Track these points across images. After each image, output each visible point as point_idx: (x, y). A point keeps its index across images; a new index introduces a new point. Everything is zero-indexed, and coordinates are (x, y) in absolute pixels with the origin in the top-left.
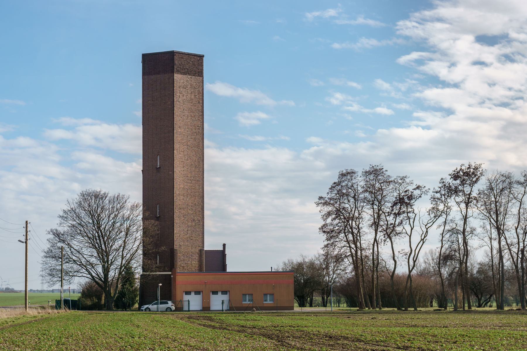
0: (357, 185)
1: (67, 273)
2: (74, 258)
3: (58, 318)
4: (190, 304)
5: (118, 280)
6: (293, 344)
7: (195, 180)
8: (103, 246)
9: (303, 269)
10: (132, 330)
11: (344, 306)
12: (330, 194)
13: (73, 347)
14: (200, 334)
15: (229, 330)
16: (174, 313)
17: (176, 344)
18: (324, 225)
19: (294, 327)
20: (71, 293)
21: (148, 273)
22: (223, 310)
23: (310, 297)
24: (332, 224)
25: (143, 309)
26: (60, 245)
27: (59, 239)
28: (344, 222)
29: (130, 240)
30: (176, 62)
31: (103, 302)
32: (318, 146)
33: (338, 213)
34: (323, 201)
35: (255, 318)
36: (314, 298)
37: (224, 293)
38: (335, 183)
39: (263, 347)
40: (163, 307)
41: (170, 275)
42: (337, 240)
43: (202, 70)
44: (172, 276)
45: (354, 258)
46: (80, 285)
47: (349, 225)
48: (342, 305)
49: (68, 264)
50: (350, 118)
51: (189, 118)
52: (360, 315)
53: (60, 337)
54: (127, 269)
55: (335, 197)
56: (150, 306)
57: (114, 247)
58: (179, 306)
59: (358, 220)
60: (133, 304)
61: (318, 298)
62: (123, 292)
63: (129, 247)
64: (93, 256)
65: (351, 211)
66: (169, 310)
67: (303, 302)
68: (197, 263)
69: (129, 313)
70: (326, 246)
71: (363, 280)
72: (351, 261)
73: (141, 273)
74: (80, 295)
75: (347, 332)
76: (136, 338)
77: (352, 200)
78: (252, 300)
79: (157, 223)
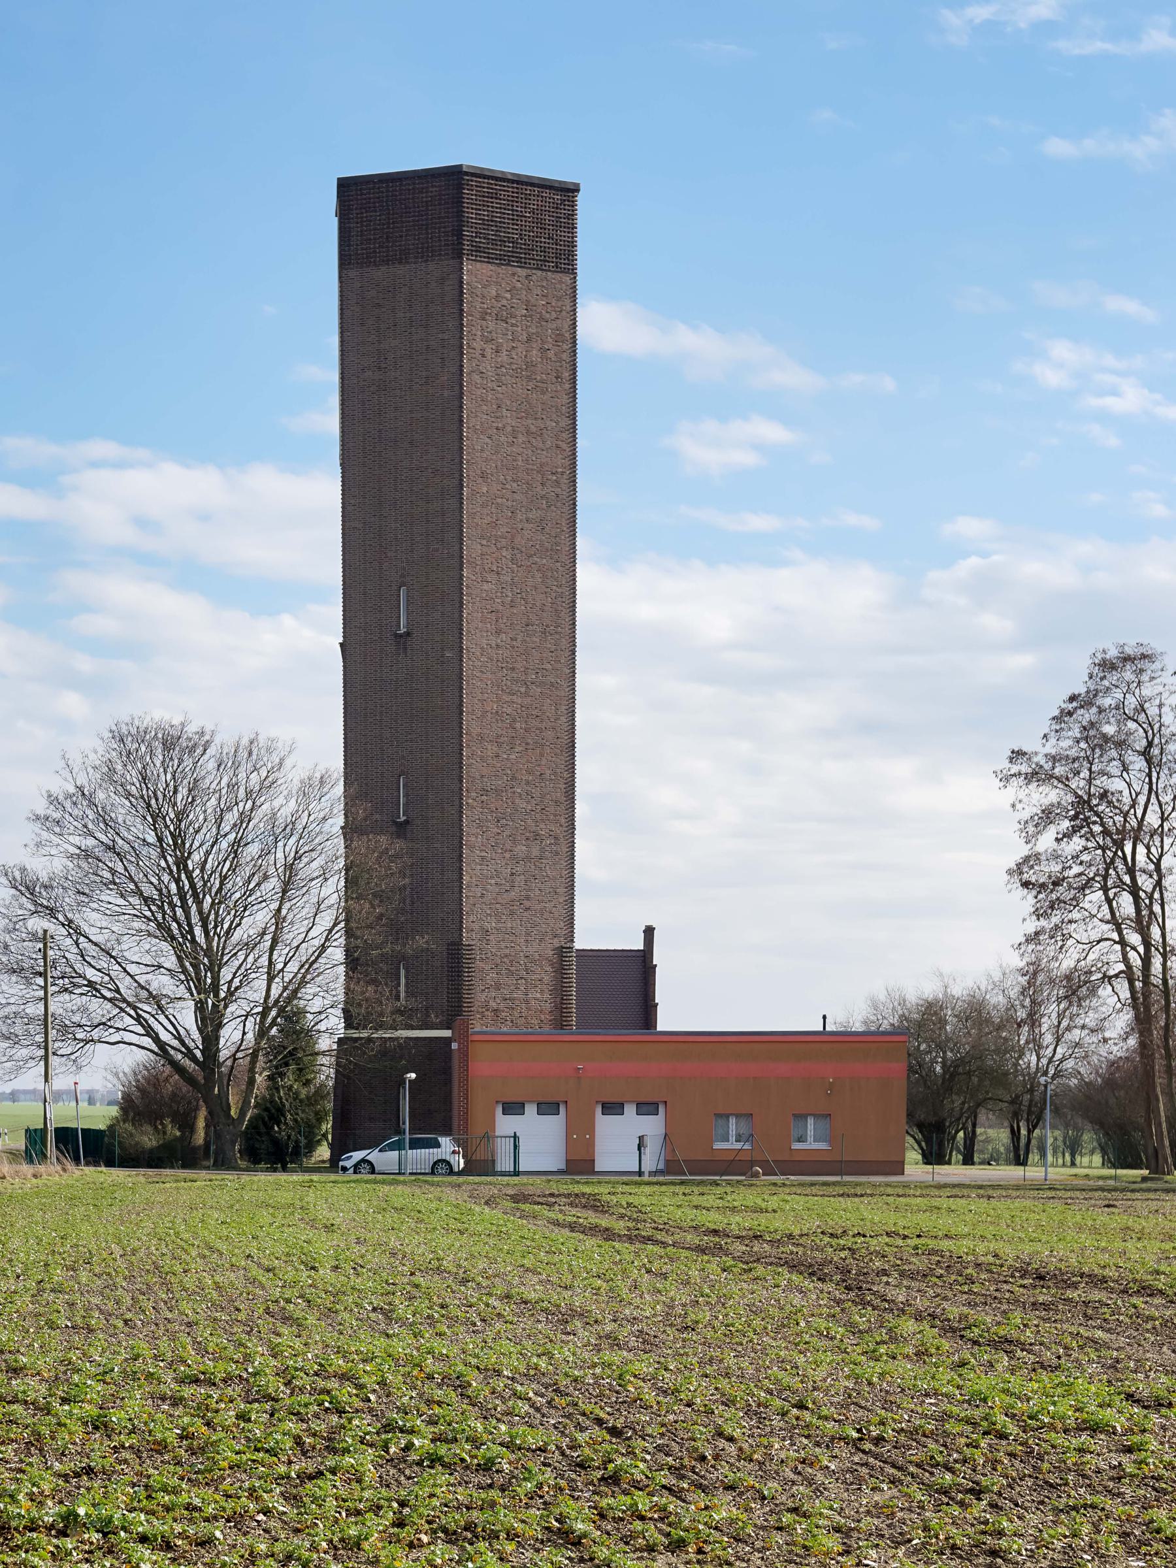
0: (1160, 706)
1: (64, 1029)
2: (91, 974)
3: (37, 1195)
4: (522, 1149)
5: (254, 1056)
6: (901, 1298)
7: (542, 684)
8: (198, 931)
9: (943, 1022)
10: (308, 1242)
11: (1092, 1164)
12: (1053, 741)
13: (96, 1300)
14: (556, 1258)
15: (664, 1244)
16: (461, 1179)
17: (470, 1292)
18: (1027, 859)
19: (905, 1237)
20: (83, 1104)
21: (364, 1034)
22: (640, 1173)
23: (964, 1128)
24: (1056, 856)
25: (348, 1164)
26: (38, 924)
27: (35, 903)
28: (1104, 849)
29: (300, 910)
30: (470, 214)
31: (200, 1137)
32: (985, 555)
33: (1083, 813)
34: (1024, 768)
35: (759, 1201)
36: (979, 1131)
37: (646, 1108)
38: (1073, 698)
39: (788, 1308)
40: (421, 1157)
41: (447, 1041)
42: (1075, 915)
43: (572, 244)
44: (454, 1046)
45: (1139, 985)
46: (116, 1075)
47: (1124, 858)
48: (1086, 1160)
49: (66, 996)
50: (1113, 441)
51: (521, 438)
52: (1151, 1195)
53: (47, 1265)
54: (288, 1019)
55: (1073, 753)
56: (374, 1156)
57: (237, 935)
58: (479, 1155)
59: (1157, 839)
60: (311, 1147)
61: (994, 1134)
62: (272, 1101)
63: (292, 935)
64: (160, 967)
65: (1133, 806)
66: (442, 1168)
67: (941, 1144)
68: (547, 996)
69: (295, 1177)
70: (1033, 938)
71: (1169, 1066)
72: (1125, 994)
73: (341, 1032)
74: (114, 1111)
75: (1104, 1258)
76: (325, 1272)
77: (1139, 763)
78: (750, 1138)
79: (399, 844)
